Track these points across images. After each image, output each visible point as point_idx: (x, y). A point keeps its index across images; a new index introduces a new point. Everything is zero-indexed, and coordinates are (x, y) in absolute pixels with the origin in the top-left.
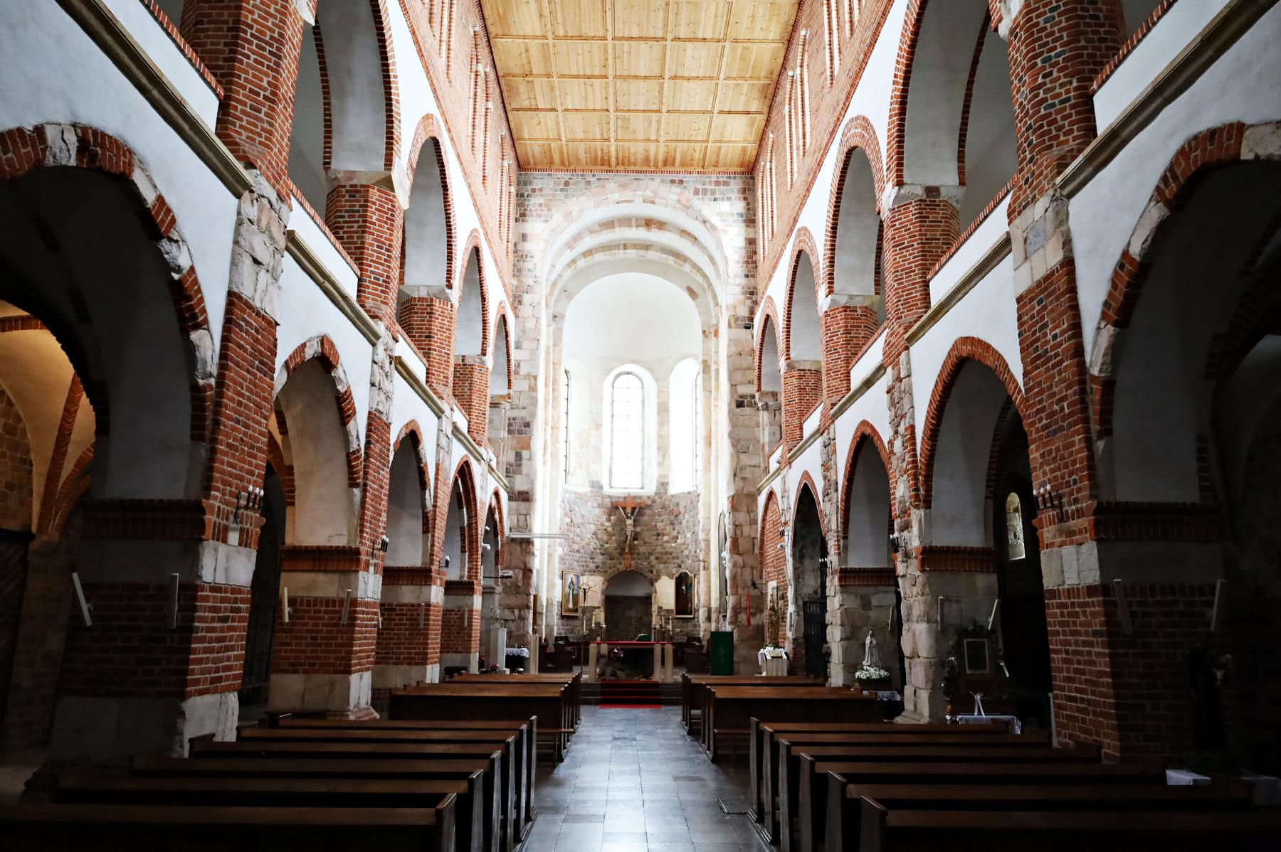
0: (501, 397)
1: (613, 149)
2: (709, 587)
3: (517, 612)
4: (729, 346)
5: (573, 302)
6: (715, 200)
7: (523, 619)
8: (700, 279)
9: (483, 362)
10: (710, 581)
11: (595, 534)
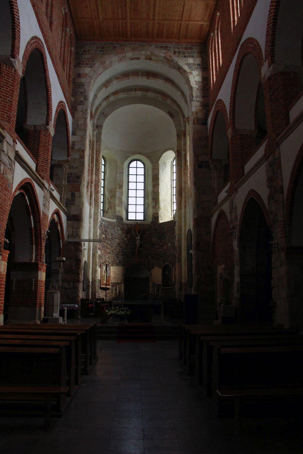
0: (64, 161)
1: (129, 25)
2: (181, 272)
3: (72, 284)
4: (194, 134)
5: (107, 120)
6: (185, 57)
7: (76, 288)
8: (175, 107)
9: (47, 130)
10: (181, 269)
11: (119, 244)
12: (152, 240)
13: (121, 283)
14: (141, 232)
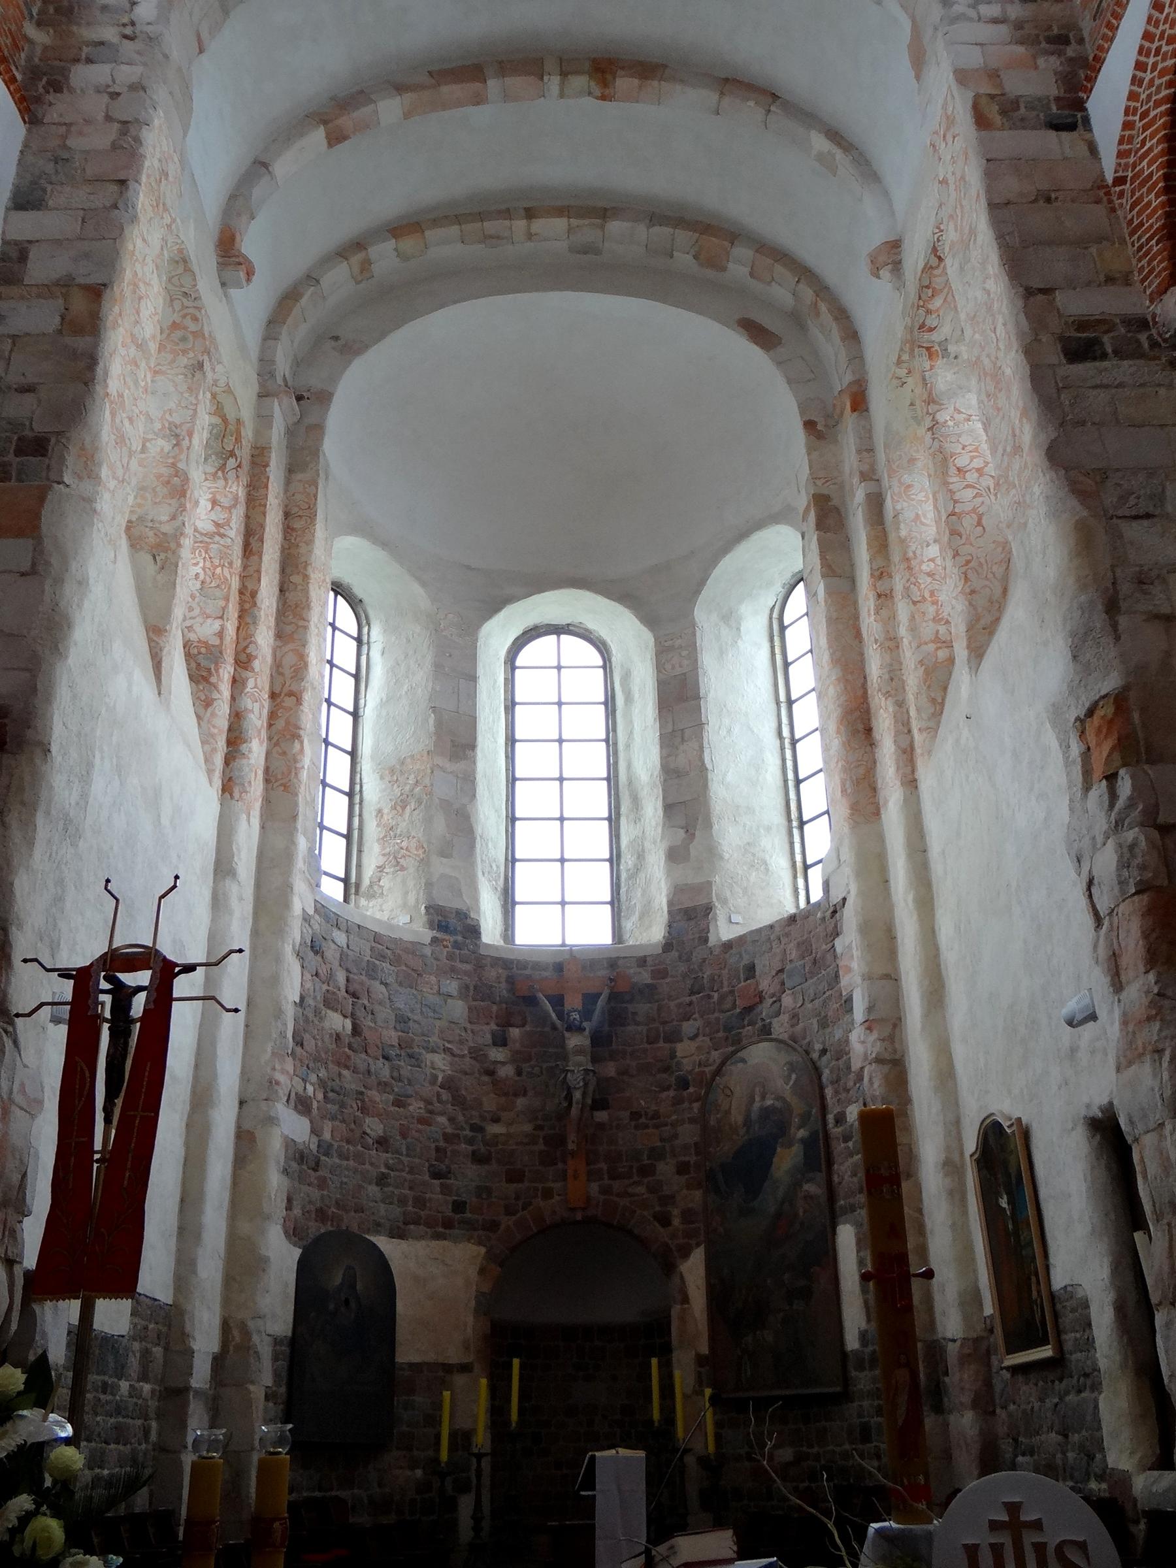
12: (673, 1055)
13: (465, 1368)
14: (601, 1002)
